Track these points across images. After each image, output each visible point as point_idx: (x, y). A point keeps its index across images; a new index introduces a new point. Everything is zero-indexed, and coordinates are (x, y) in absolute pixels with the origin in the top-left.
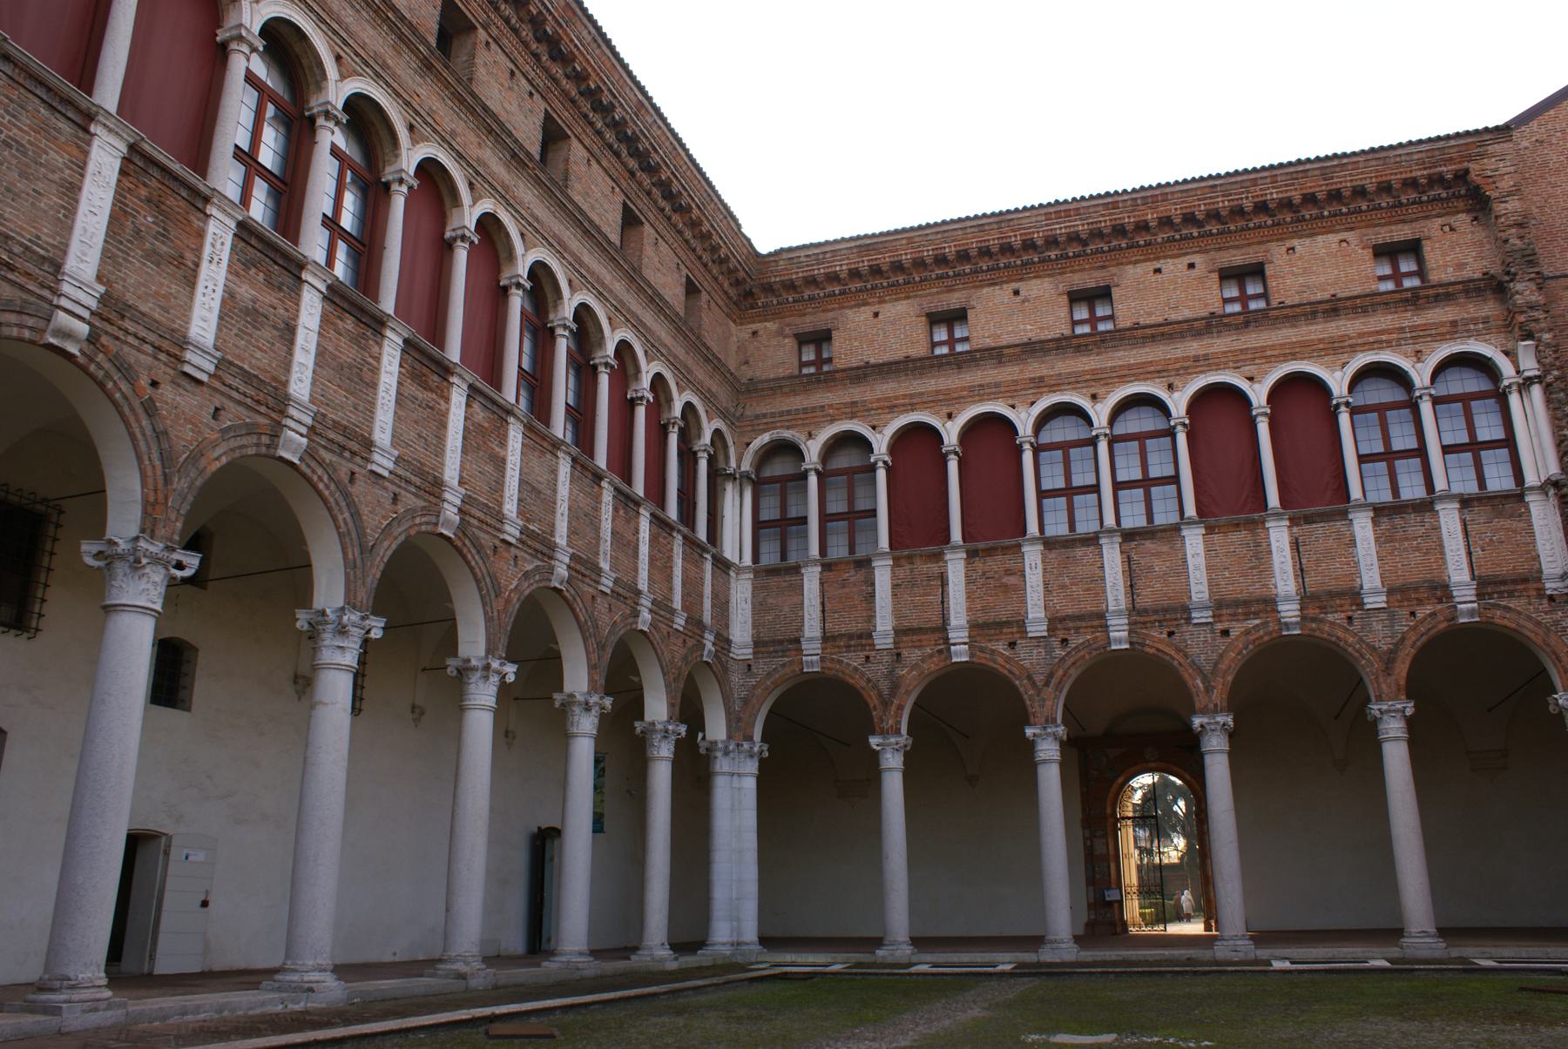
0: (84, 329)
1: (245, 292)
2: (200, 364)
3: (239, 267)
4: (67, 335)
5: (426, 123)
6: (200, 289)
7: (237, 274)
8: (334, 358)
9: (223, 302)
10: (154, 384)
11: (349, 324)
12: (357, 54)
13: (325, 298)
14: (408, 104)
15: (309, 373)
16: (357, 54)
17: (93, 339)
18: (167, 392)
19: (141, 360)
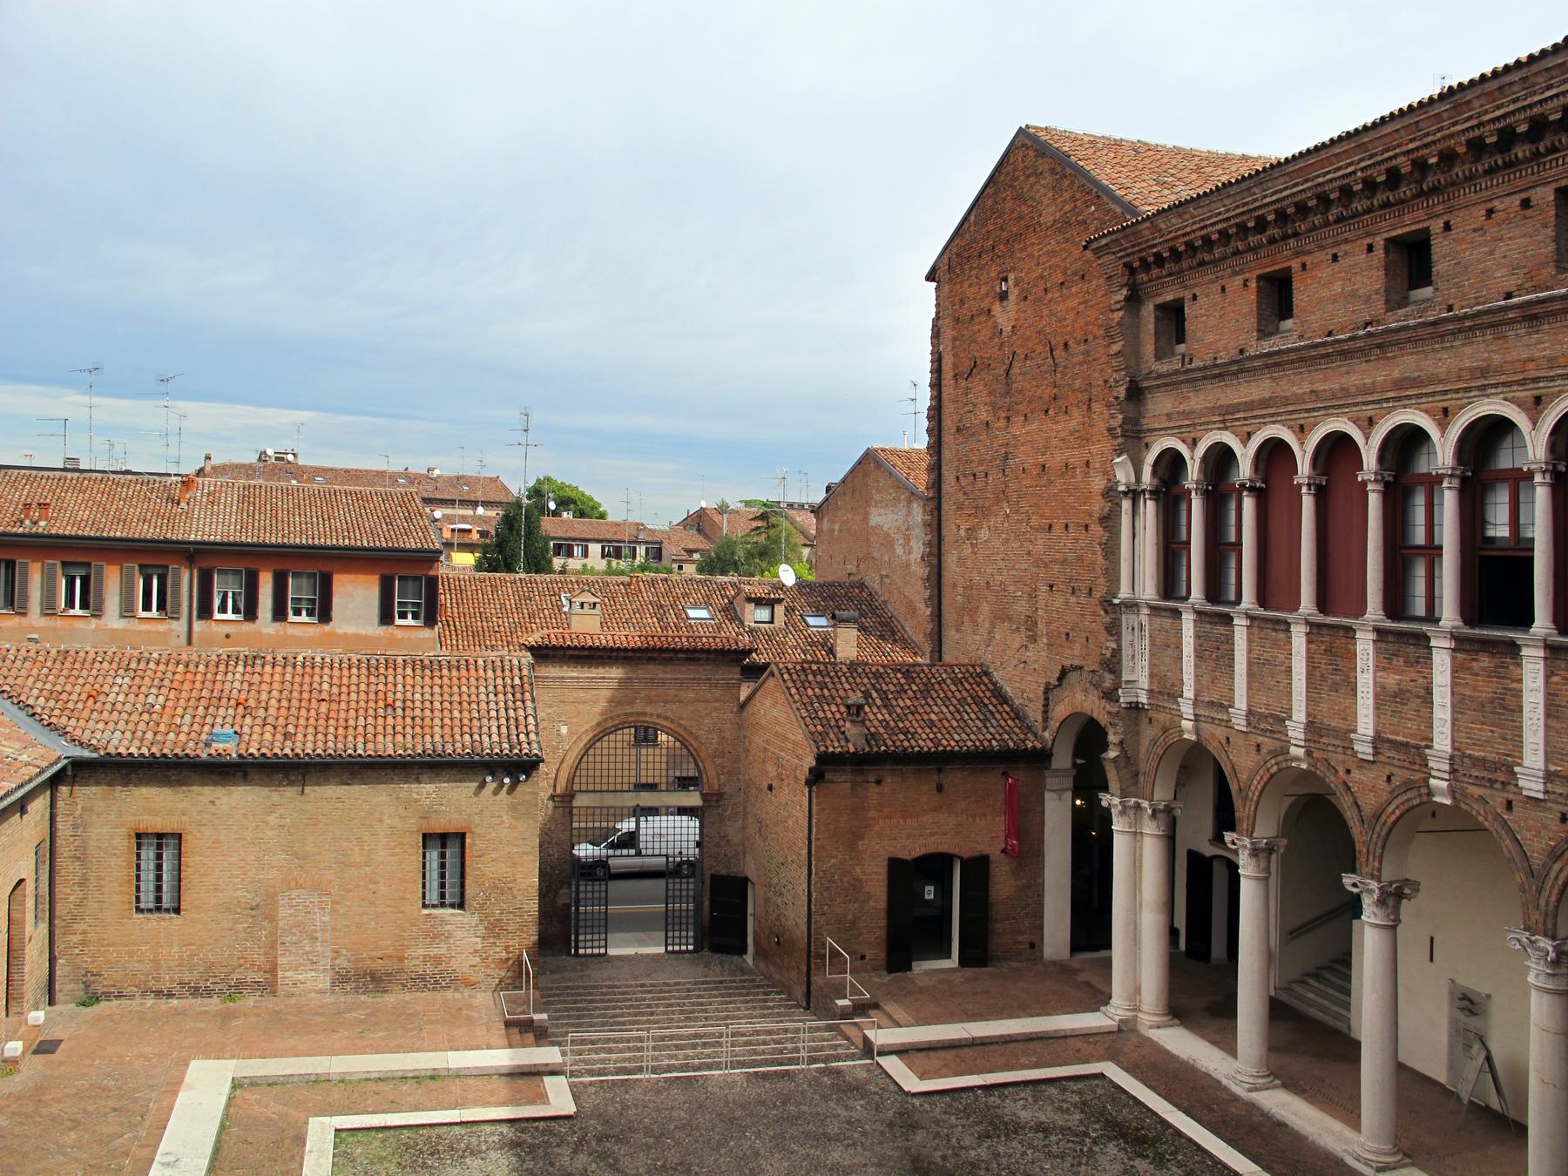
0: (1300, 752)
1: (1392, 680)
2: (1364, 750)
3: (1385, 663)
4: (1298, 759)
5: (1552, 379)
6: (1359, 695)
7: (1384, 669)
8: (1473, 699)
9: (1376, 696)
10: (1348, 771)
11: (1485, 661)
12: (1457, 391)
13: (1454, 650)
14: (1518, 383)
15: (1449, 724)
16: (1457, 391)
17: (1309, 753)
18: (1356, 774)
19: (1336, 758)
